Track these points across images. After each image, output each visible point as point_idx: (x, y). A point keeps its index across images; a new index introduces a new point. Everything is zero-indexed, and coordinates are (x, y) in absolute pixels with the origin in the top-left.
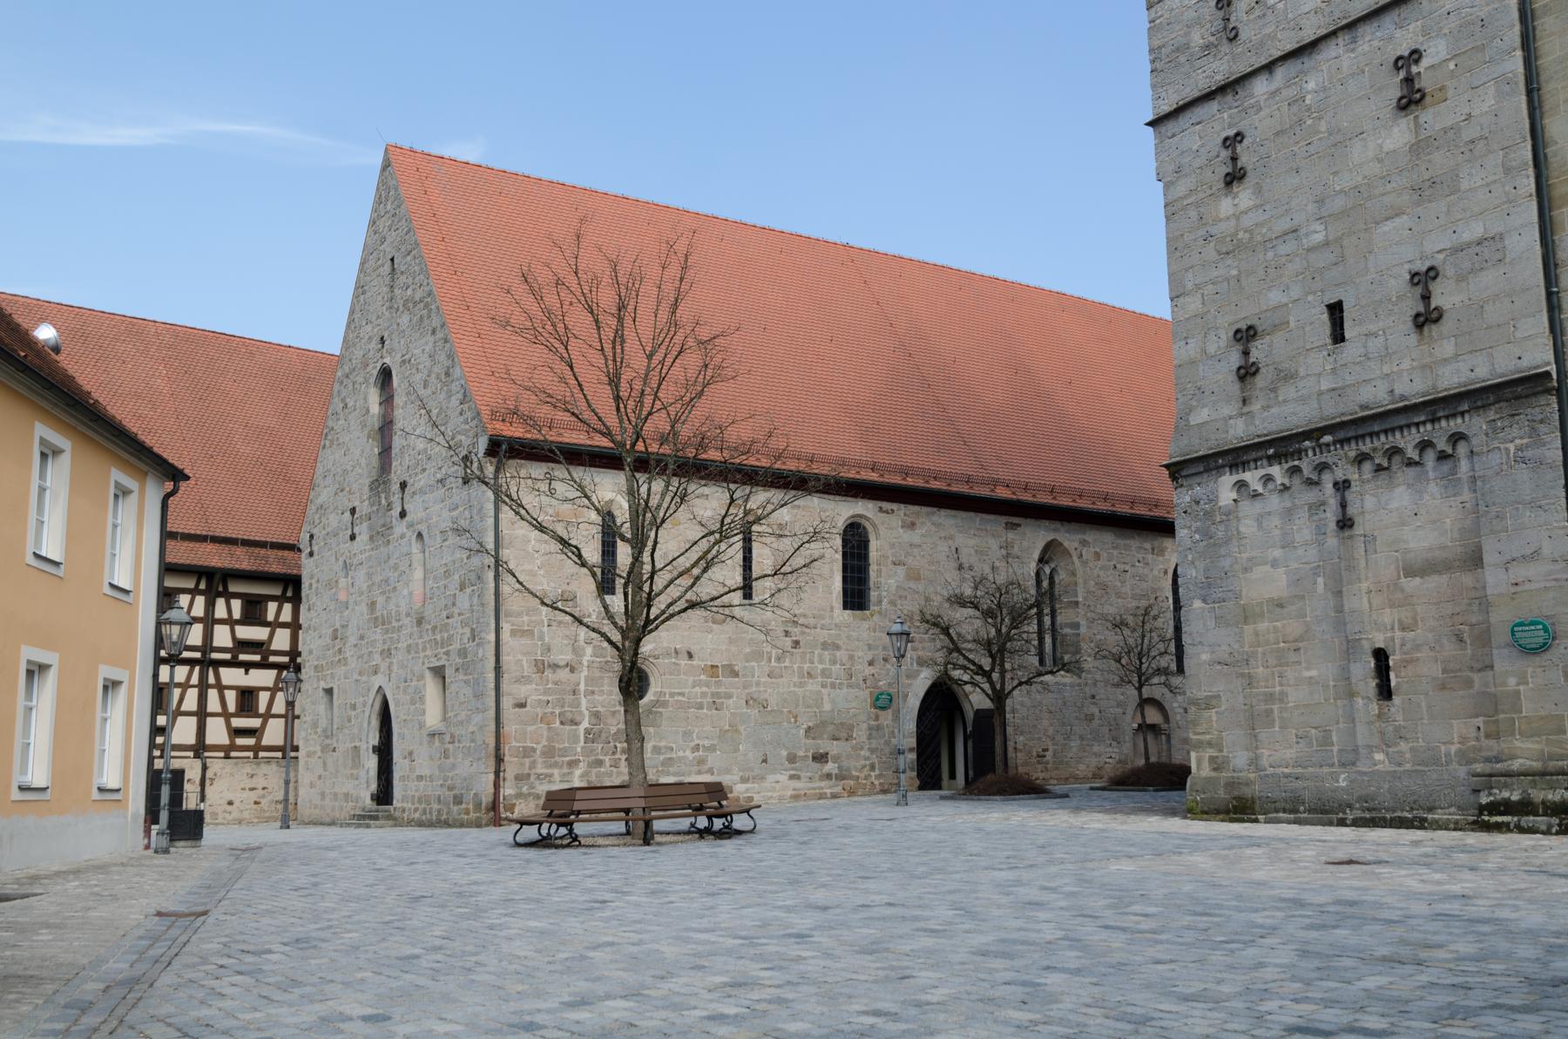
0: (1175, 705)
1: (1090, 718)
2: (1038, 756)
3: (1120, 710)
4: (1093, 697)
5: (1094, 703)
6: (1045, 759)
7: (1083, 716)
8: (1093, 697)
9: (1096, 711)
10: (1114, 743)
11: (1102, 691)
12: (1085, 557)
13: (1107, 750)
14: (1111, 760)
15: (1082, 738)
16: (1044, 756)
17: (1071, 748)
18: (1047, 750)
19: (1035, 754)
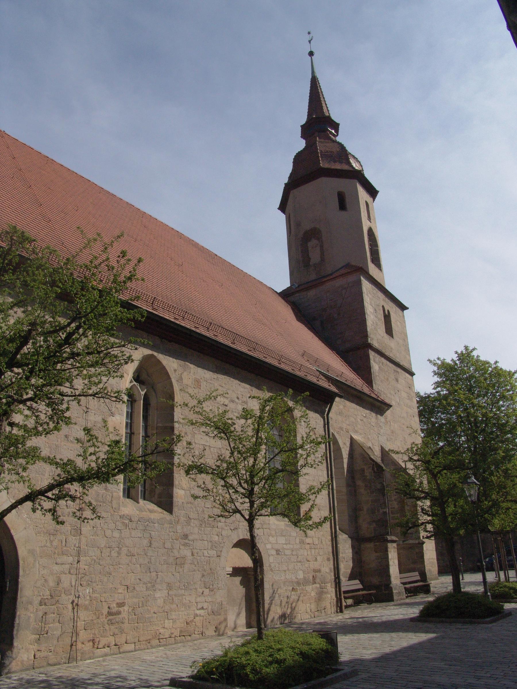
0: (269, 546)
1: (180, 562)
2: (110, 614)
3: (213, 553)
4: (186, 536)
5: (185, 545)
6: (118, 618)
7: (171, 560)
8: (186, 536)
9: (187, 552)
10: (207, 591)
11: (196, 530)
12: (185, 381)
13: (199, 599)
14: (202, 612)
15: (169, 586)
16: (119, 613)
17: (155, 599)
18: (121, 605)
19: (105, 611)
